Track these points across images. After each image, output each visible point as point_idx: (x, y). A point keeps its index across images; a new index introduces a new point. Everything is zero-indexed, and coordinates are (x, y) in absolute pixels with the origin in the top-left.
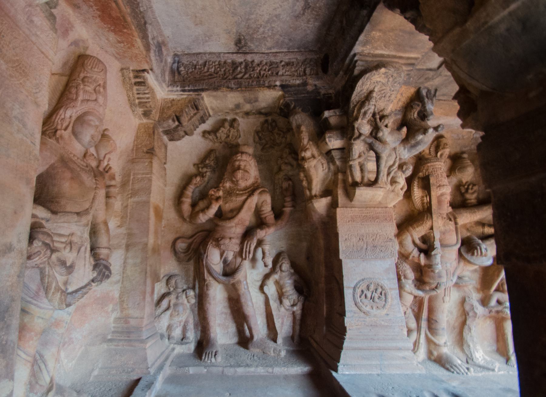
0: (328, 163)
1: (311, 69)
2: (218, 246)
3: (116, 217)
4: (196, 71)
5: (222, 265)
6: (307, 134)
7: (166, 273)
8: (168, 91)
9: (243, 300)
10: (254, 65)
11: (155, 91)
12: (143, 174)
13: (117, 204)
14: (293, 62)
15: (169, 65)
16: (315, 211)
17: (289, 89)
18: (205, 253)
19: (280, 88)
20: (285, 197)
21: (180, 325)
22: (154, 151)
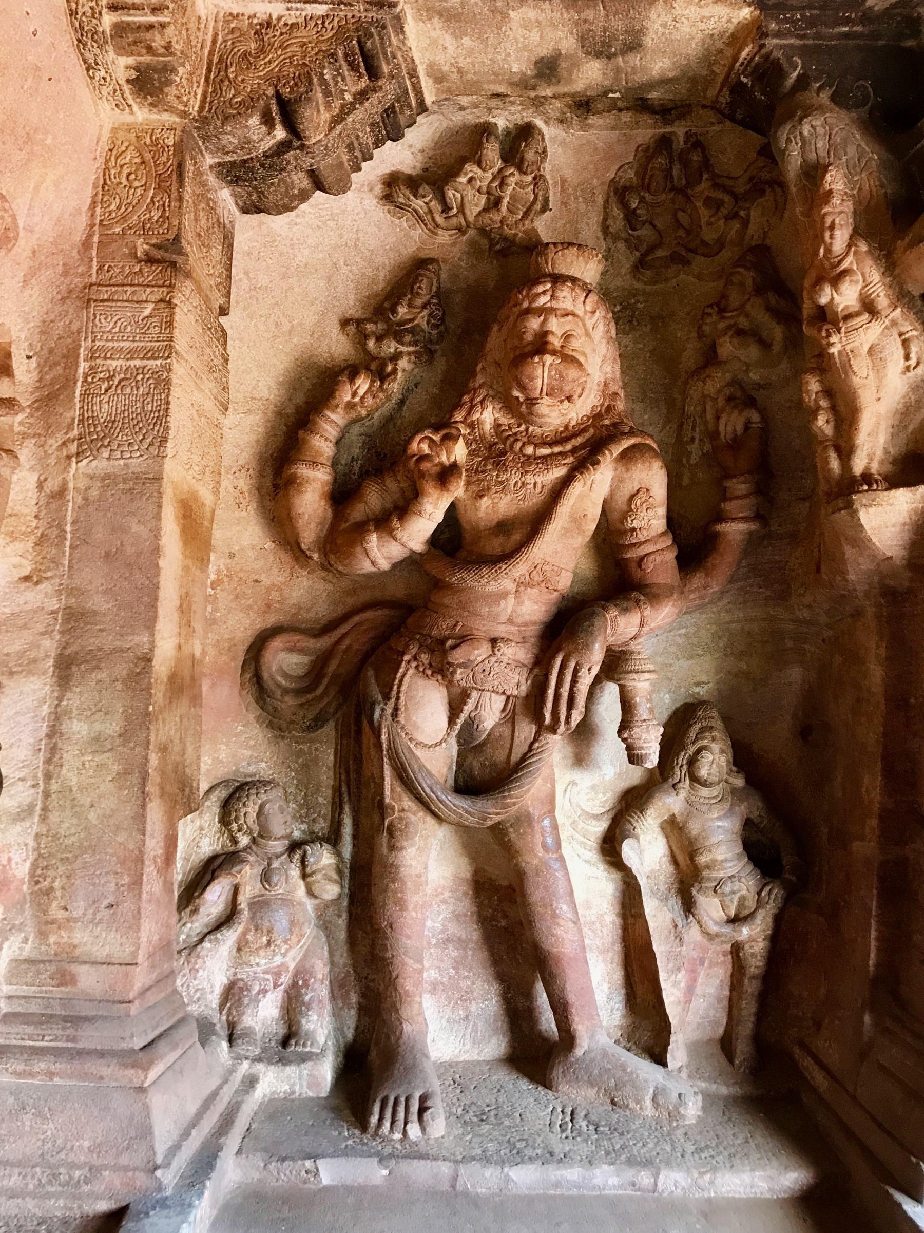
2: (441, 669)
6: (849, 206)
7: (222, 772)
9: (536, 895)
12: (131, 354)
16: (858, 538)
18: (387, 697)
20: (728, 476)
21: (276, 986)
22: (180, 252)
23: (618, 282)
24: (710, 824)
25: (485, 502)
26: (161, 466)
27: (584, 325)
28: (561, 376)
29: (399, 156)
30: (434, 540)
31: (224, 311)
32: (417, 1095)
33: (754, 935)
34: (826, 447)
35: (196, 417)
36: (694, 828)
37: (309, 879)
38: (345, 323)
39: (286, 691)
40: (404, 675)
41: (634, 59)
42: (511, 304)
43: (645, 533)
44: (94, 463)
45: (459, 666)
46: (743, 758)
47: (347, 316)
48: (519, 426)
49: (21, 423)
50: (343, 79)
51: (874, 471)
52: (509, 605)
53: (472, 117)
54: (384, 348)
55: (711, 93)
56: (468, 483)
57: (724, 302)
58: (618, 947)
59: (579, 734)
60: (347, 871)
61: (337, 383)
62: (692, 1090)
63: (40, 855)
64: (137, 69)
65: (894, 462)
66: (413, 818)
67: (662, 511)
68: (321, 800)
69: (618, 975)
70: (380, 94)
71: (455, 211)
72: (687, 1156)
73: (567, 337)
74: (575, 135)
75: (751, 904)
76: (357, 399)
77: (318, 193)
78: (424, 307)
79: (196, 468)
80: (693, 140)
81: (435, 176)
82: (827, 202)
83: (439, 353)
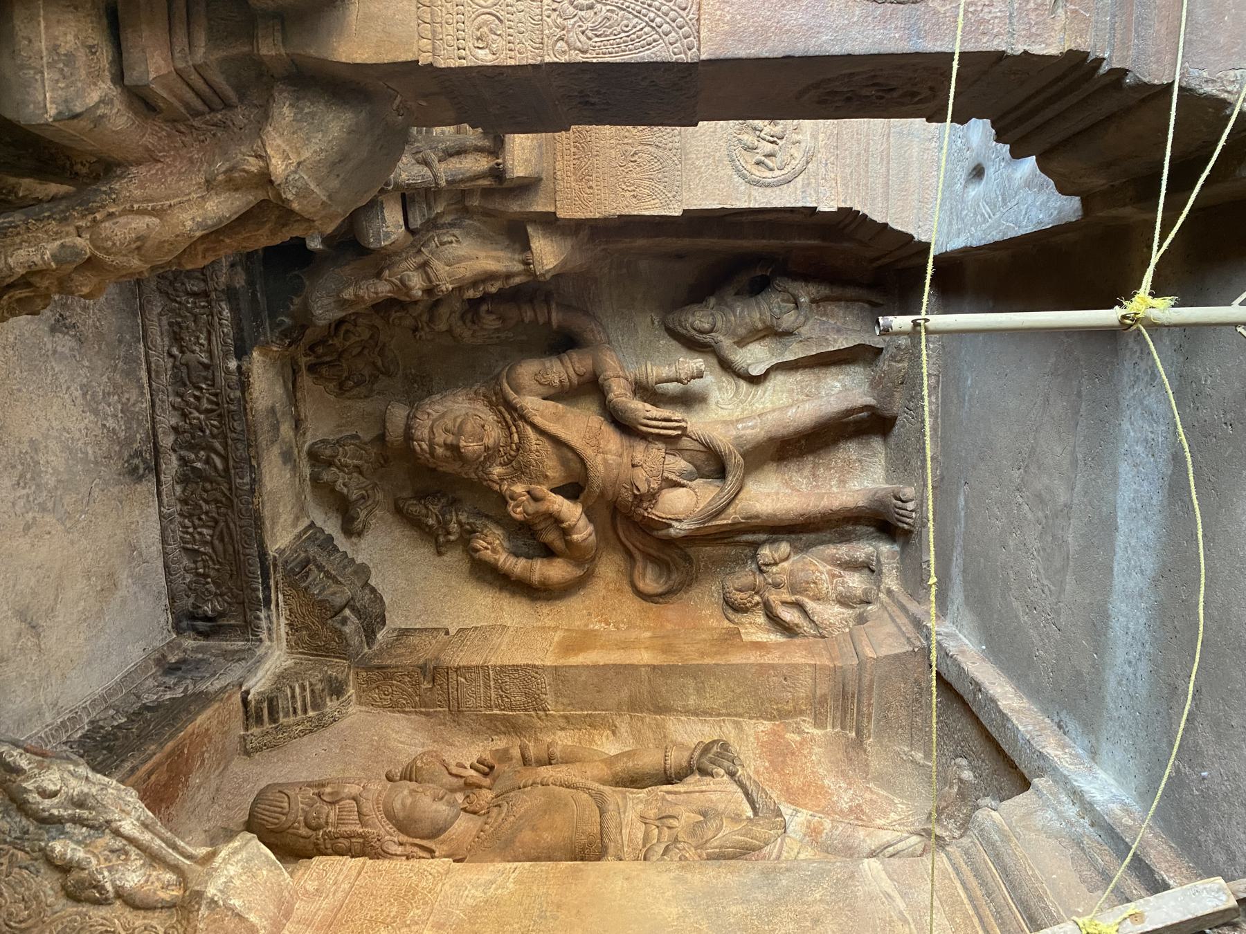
0: (436, 227)
2: (653, 496)
3: (592, 741)
6: (364, 284)
7: (718, 612)
8: (271, 640)
10: (187, 426)
12: (487, 687)
13: (563, 740)
17: (245, 334)
19: (245, 358)
21: (841, 576)
29: (331, 526)
31: (447, 633)
36: (741, 331)
38: (440, 554)
39: (669, 578)
52: (611, 458)
56: (539, 483)
58: (816, 371)
61: (480, 560)
69: (833, 370)
73: (447, 431)
75: (786, 296)
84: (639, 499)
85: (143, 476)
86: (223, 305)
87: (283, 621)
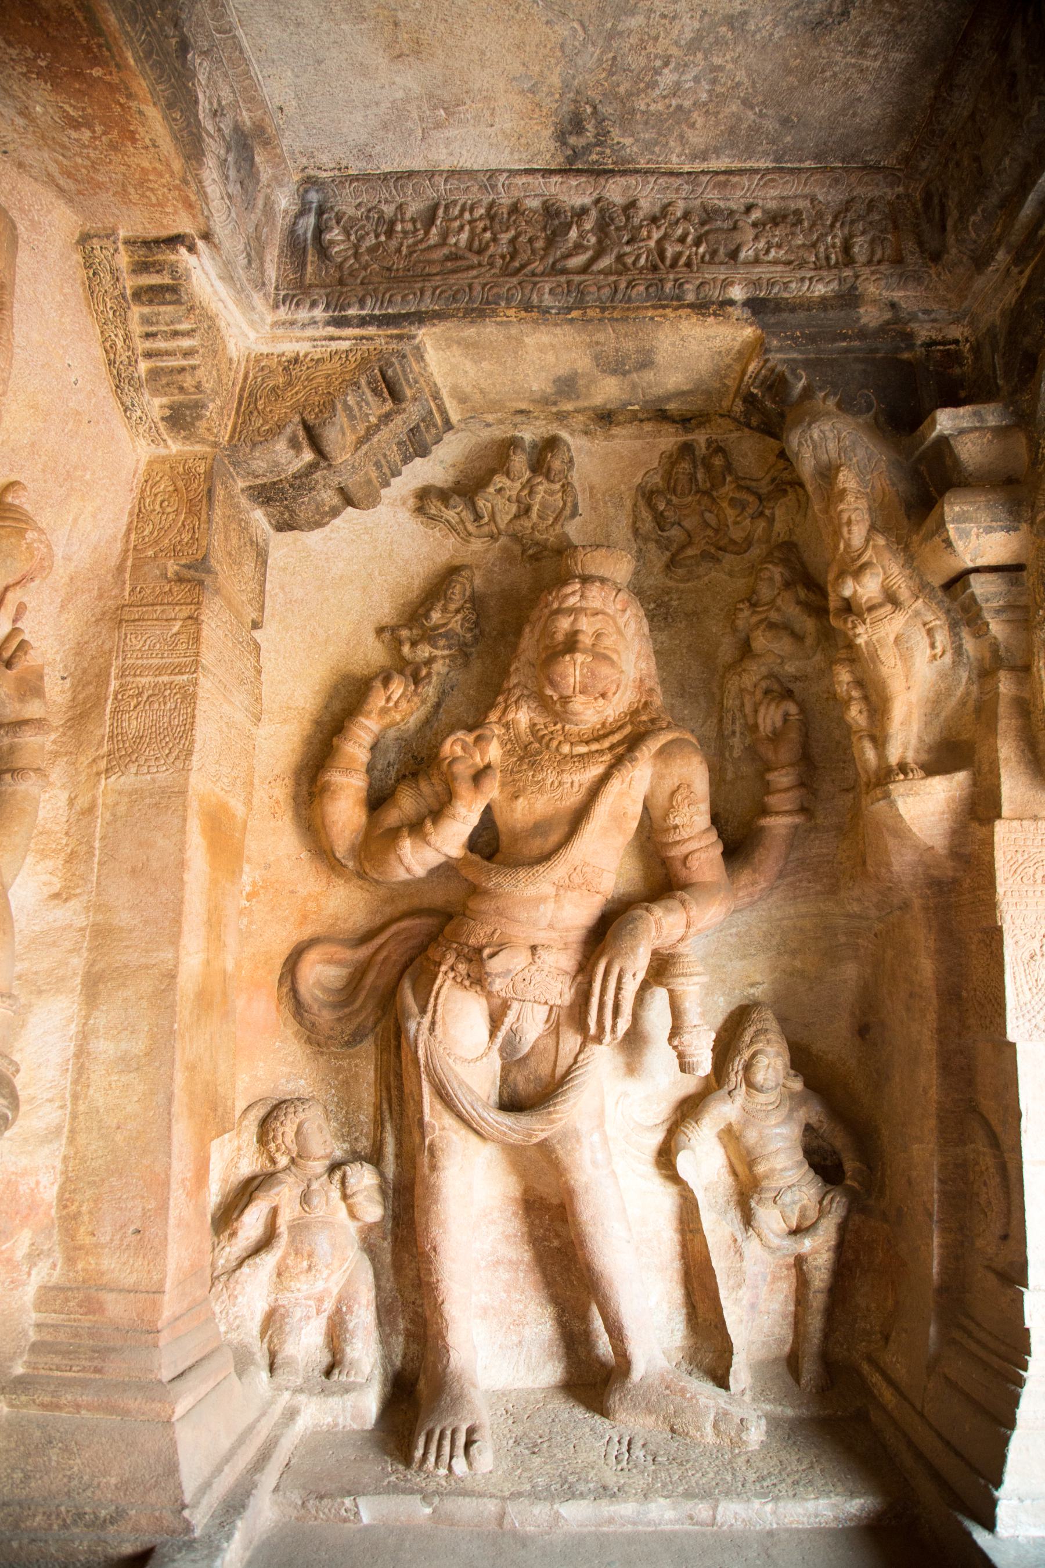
0: (953, 626)
1: (872, 242)
2: (478, 980)
3: (43, 854)
4: (394, 244)
5: (497, 1063)
6: (863, 504)
7: (261, 1089)
8: (275, 324)
10: (636, 221)
11: (223, 324)
12: (160, 670)
14: (797, 212)
15: (281, 223)
16: (900, 830)
17: (785, 315)
18: (423, 1011)
19: (747, 313)
22: (209, 571)
23: (651, 581)
24: (767, 1131)
25: (521, 803)
26: (187, 779)
27: (615, 623)
28: (593, 674)
29: (433, 469)
30: (474, 844)
31: (256, 625)
32: (464, 1428)
33: (819, 1248)
34: (861, 737)
35: (225, 729)
36: (751, 1137)
37: (350, 1201)
38: (380, 631)
39: (323, 1005)
40: (440, 988)
41: (649, 376)
42: (543, 604)
43: (688, 830)
44: (123, 778)
45: (498, 975)
46: (801, 1059)
47: (383, 624)
48: (555, 724)
49: (54, 742)
50: (367, 404)
51: (909, 760)
52: (547, 910)
53: (498, 433)
54: (419, 653)
55: (726, 404)
56: (503, 785)
57: (755, 597)
58: (677, 1265)
59: (630, 1042)
60: (390, 1192)
62: (755, 1414)
63: (68, 1178)
64: (171, 408)
65: (930, 750)
66: (455, 1137)
67: (705, 807)
68: (362, 1117)
69: (678, 1294)
70: (404, 416)
71: (486, 519)
72: (747, 1485)
73: (598, 635)
74: (599, 445)
75: (812, 1214)
76: (391, 704)
77: (350, 509)
78: (458, 611)
79: (225, 780)
80: (714, 445)
81: (467, 488)
82: (841, 501)
83: (475, 655)
84: (475, 957)
85: (564, 143)
86: (835, 285)
87: (303, 348)
